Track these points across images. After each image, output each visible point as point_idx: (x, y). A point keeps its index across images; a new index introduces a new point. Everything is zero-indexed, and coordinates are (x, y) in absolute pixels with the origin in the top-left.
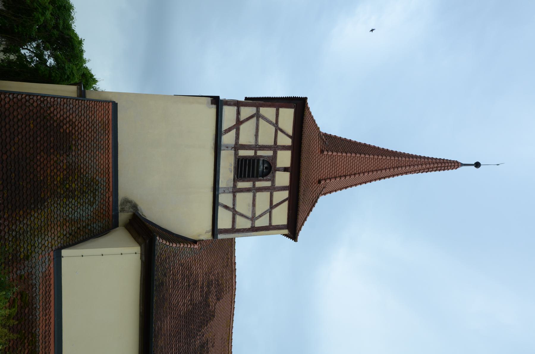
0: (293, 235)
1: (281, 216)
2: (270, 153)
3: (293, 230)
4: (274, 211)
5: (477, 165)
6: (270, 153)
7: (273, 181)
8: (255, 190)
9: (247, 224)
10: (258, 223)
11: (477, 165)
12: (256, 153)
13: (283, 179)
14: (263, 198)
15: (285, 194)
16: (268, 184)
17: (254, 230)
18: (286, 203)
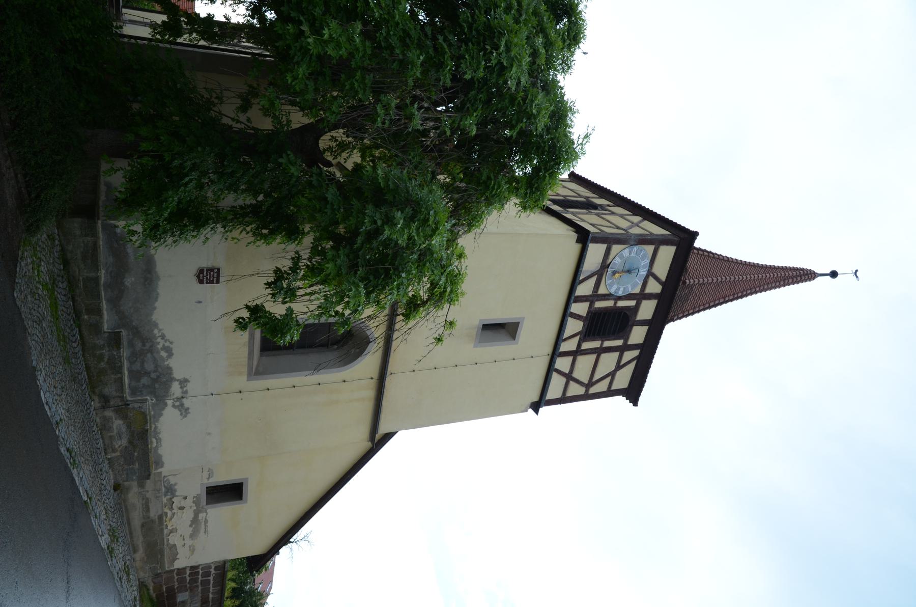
0: (634, 400)
1: (623, 379)
2: (632, 303)
5: (834, 274)
6: (632, 303)
7: (626, 339)
8: (599, 352)
9: (581, 391)
10: (593, 390)
11: (834, 274)
12: (615, 303)
13: (638, 335)
14: (608, 361)
15: (636, 353)
16: (619, 343)
17: (587, 397)
18: (634, 363)
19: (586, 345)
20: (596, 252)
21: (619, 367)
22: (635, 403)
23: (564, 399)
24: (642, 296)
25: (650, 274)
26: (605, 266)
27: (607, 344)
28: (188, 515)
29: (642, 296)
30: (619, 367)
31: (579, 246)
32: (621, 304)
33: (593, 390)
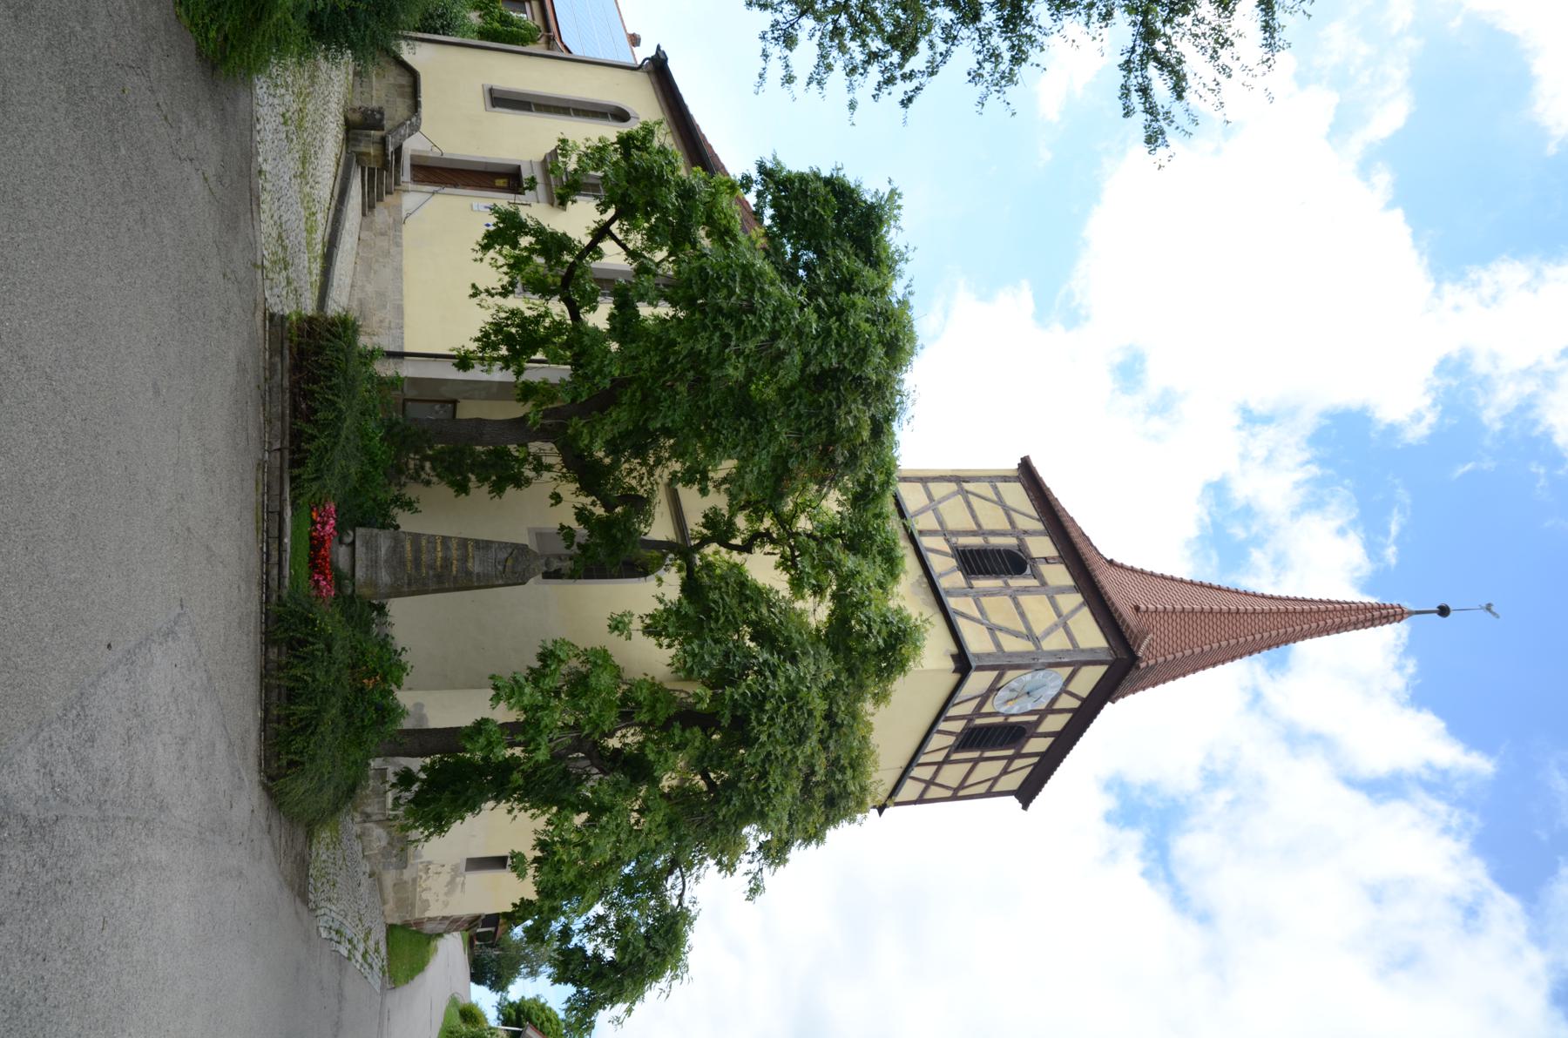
1: (1014, 780)
3: (1026, 794)
4: (1004, 778)
14: (992, 769)
16: (1010, 752)
19: (955, 757)
20: (978, 681)
21: (1005, 772)
22: (1025, 807)
23: (921, 800)
24: (1050, 710)
25: (1064, 690)
26: (993, 689)
27: (988, 754)
28: (445, 877)
29: (1050, 710)
30: (1005, 772)
31: (956, 677)
32: (1012, 720)
33: (961, 793)
